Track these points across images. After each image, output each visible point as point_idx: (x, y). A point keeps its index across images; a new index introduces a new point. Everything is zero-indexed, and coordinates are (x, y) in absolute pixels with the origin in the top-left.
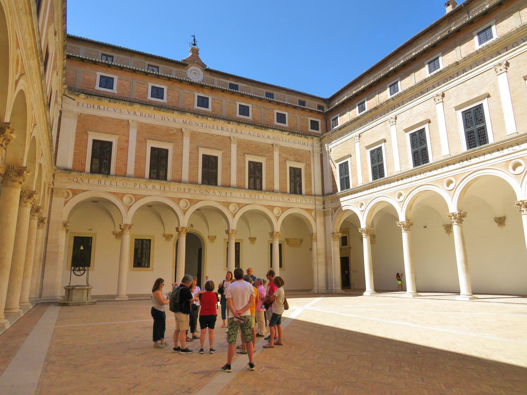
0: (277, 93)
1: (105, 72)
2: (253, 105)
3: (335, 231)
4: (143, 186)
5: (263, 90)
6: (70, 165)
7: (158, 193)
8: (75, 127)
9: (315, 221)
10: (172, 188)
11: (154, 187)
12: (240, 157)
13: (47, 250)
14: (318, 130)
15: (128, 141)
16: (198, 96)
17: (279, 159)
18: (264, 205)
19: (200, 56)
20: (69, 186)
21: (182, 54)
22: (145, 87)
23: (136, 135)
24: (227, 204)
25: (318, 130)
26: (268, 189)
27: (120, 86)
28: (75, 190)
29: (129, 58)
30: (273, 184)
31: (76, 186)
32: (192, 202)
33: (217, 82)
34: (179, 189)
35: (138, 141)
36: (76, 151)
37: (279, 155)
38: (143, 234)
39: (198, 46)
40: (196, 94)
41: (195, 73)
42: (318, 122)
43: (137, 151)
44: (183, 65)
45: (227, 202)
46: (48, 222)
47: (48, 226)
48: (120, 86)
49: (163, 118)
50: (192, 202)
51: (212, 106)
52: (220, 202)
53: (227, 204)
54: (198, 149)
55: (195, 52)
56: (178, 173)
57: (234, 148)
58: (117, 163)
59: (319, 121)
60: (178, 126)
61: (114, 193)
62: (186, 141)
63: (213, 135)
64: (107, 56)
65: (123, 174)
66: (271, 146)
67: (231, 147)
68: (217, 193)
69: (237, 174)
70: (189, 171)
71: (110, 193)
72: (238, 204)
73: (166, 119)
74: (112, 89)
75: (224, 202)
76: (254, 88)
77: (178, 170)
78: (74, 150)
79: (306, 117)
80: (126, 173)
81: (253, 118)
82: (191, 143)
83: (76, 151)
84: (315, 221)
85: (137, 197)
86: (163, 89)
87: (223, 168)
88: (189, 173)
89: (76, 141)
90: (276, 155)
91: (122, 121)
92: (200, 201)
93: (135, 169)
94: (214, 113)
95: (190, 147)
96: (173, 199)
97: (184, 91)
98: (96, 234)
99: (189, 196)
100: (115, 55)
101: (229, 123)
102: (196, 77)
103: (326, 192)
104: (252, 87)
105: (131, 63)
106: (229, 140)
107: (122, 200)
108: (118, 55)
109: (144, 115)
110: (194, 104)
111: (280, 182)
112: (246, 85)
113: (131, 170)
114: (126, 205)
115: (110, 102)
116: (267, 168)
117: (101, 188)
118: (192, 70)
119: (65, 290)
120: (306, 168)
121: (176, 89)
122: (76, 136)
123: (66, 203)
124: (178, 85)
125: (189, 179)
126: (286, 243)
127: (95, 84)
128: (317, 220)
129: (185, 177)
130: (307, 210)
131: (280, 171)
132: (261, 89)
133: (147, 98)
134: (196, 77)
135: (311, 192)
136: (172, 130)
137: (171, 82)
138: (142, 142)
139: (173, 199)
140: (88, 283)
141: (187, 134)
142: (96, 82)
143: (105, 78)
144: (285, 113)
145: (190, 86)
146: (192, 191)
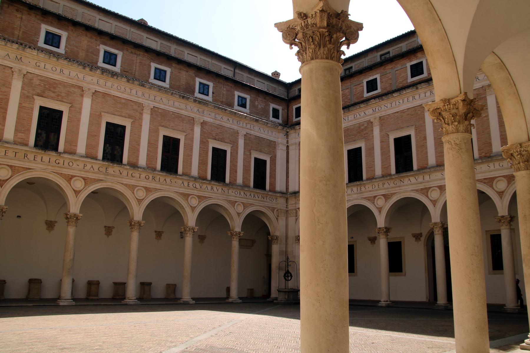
7: (355, 196)
10: (367, 187)
11: (352, 190)
24: (425, 191)
29: (363, 60)
34: (374, 186)
38: (394, 236)
45: (426, 188)
50: (387, 197)
52: (417, 190)
54: (388, 135)
56: (372, 169)
60: (367, 118)
63: (403, 111)
68: (413, 180)
73: (358, 116)
75: (422, 189)
77: (371, 167)
82: (381, 131)
87: (417, 147)
88: (382, 166)
92: (395, 193)
97: (396, 69)
98: (356, 241)
99: (383, 192)
100: (353, 65)
101: (417, 88)
108: (356, 63)
110: (407, 79)
121: (388, 72)
124: (389, 66)
125: (382, 171)
129: (378, 172)
136: (363, 125)
137: (383, 67)
145: (401, 60)
146: (386, 185)
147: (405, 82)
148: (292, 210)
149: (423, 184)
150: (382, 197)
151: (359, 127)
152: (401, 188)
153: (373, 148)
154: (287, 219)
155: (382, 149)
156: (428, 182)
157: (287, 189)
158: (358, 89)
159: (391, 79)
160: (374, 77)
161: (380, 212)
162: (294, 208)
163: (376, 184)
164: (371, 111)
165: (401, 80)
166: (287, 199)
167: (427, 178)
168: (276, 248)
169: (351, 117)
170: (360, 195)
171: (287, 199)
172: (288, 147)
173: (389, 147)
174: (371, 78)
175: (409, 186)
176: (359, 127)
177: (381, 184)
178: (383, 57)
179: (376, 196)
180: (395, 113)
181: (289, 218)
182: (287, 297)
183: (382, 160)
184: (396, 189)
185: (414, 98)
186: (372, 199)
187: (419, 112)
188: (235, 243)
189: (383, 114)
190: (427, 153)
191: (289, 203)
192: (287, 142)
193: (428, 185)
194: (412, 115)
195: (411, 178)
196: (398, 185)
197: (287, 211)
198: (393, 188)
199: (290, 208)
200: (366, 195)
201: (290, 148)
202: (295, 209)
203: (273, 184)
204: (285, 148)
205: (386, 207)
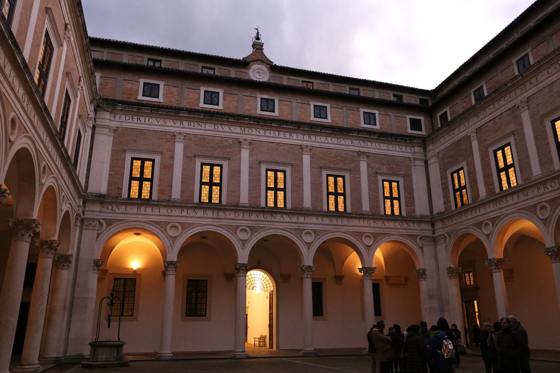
0: (364, 88)
1: (149, 78)
2: (331, 105)
3: (452, 266)
4: (191, 212)
5: (346, 85)
6: (103, 190)
8: (111, 144)
9: (422, 251)
12: (314, 170)
13: (75, 296)
14: (421, 130)
15: (172, 158)
16: (262, 99)
17: (368, 169)
18: (350, 232)
19: (265, 51)
20: (103, 216)
21: (242, 52)
22: (196, 93)
23: (182, 149)
24: (299, 232)
25: (421, 130)
26: (355, 210)
27: (167, 94)
28: (110, 220)
30: (360, 203)
31: (111, 216)
32: (253, 230)
33: (285, 81)
34: (237, 214)
35: (185, 156)
36: (111, 173)
37: (368, 165)
39: (263, 40)
40: (259, 96)
41: (259, 72)
42: (420, 120)
43: (184, 169)
44: (244, 64)
46: (77, 260)
47: (77, 265)
48: (167, 94)
49: (216, 127)
50: (253, 230)
51: (280, 110)
52: (290, 229)
53: (299, 232)
54: (260, 162)
55: (258, 46)
57: (306, 159)
58: (159, 185)
59: (422, 118)
61: (156, 222)
62: (245, 154)
64: (154, 61)
65: (167, 198)
66: (356, 154)
67: (302, 158)
69: (312, 192)
70: (249, 190)
71: (152, 221)
72: (315, 231)
74: (158, 97)
76: (334, 84)
78: (110, 171)
79: (404, 115)
80: (171, 196)
81: (332, 120)
82: (250, 155)
83: (112, 173)
84: (422, 251)
85: (185, 226)
86: (218, 93)
89: (112, 161)
90: (363, 166)
91: (167, 133)
93: (182, 192)
94: (281, 118)
95: (250, 160)
96: (229, 228)
99: (249, 223)
100: (164, 59)
102: (260, 77)
103: (435, 212)
104: (331, 84)
105: (182, 66)
106: (300, 150)
107: (166, 230)
109: (192, 124)
110: (256, 109)
111: (370, 201)
112: (323, 82)
113: (176, 194)
114: (171, 237)
115: (151, 110)
116: (351, 182)
117: (140, 216)
118: (254, 70)
119: (90, 347)
120: (405, 181)
122: (112, 155)
123: (98, 235)
125: (249, 200)
126: (385, 282)
127: (138, 93)
128: (425, 249)
130: (410, 236)
131: (369, 186)
132: (342, 85)
133: (198, 106)
134: (260, 77)
135: (414, 211)
136: (226, 141)
138: (190, 157)
139: (229, 228)
140: (119, 339)
142: (138, 90)
143: (150, 86)
144: (374, 111)
147: (253, 111)
148: (93, 220)
149: (297, 225)
151: (222, 142)
152: (272, 223)
153: (239, 171)
155: (250, 175)
156: (303, 223)
158: (192, 94)
159: (237, 101)
160: (216, 90)
161: (244, 245)
162: (98, 217)
163: (241, 214)
164: (238, 130)
165: (249, 108)
166: (84, 203)
167: (302, 219)
169: (209, 126)
170: (217, 220)
172: (94, 127)
173: (260, 175)
174: (211, 89)
175: (282, 224)
176: (222, 142)
177: (247, 216)
178: (205, 71)
179: (240, 226)
180: (270, 142)
181: (84, 232)
182: (115, 355)
183: (250, 187)
184: (267, 223)
185: (291, 135)
186: (234, 229)
187: (297, 152)
189: (255, 138)
190: (302, 194)
191: (87, 208)
193: (302, 226)
194: (289, 152)
195: (284, 216)
196: (268, 219)
197: (83, 220)
198: (263, 221)
199: (86, 216)
200: (225, 222)
201: (97, 130)
205: (252, 241)
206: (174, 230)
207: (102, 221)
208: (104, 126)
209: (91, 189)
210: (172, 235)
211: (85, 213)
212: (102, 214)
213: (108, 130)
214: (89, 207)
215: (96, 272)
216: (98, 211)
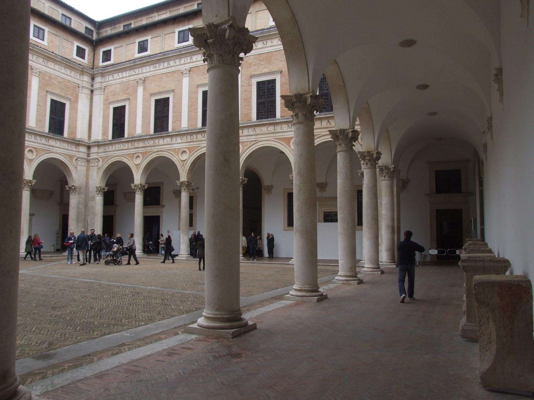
77: (178, 118)
107: (133, 160)
141: (185, 75)
150: (187, 150)
154: (88, 170)
157: (90, 137)
162: (96, 157)
166: (89, 148)
168: (74, 200)
171: (89, 148)
172: (92, 91)
188: (26, 195)
192: (92, 85)
201: (95, 92)
202: (98, 159)
203: (73, 131)
204: (89, 92)
206: (138, 159)
207: (100, 159)
208: (98, 89)
209: (94, 138)
210: (136, 163)
211: (91, 155)
212: (99, 154)
213: (100, 90)
214: (94, 150)
215: (100, 195)
216: (95, 153)
